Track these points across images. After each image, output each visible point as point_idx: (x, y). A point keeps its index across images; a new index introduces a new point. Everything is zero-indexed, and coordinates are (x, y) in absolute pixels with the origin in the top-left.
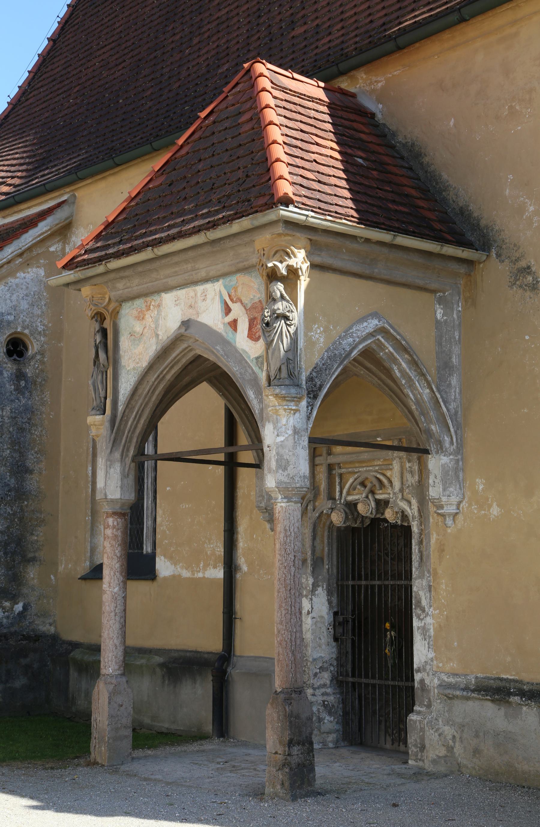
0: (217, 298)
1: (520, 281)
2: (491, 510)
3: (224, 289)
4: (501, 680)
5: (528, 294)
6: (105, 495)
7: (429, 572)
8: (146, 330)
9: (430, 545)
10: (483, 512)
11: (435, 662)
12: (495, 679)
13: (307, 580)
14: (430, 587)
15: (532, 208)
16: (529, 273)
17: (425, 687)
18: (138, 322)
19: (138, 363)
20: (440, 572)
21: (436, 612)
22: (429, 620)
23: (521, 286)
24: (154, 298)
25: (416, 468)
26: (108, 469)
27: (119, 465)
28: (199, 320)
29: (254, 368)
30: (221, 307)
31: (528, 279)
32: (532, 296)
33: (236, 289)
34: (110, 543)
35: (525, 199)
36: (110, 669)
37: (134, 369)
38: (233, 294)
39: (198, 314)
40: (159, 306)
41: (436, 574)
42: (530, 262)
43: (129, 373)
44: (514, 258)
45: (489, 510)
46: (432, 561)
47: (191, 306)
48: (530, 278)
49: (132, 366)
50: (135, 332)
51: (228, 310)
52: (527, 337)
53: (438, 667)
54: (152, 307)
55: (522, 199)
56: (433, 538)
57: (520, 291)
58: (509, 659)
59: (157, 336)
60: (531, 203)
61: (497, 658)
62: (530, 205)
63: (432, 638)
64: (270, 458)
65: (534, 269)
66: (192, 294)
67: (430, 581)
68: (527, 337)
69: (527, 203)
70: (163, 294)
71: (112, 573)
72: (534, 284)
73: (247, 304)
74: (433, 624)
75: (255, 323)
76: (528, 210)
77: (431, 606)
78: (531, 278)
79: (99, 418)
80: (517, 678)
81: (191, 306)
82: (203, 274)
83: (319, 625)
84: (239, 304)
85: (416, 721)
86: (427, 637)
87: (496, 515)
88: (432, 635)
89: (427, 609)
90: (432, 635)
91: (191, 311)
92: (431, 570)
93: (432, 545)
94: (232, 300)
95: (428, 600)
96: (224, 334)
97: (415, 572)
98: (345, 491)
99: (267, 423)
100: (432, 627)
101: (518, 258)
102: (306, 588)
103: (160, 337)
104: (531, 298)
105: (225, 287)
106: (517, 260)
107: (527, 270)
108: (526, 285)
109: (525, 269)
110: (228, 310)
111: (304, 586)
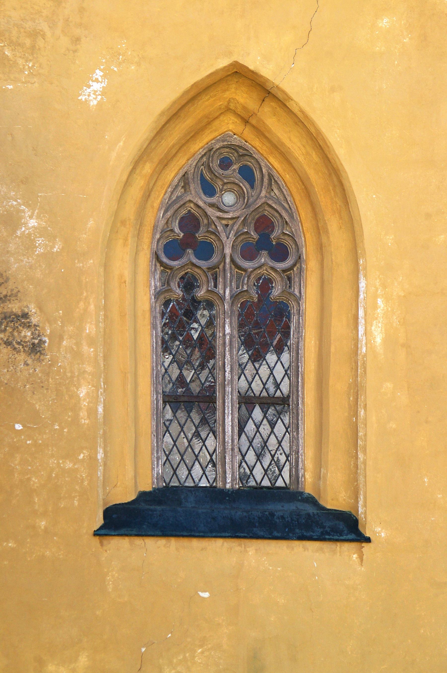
1: (7, 334)
5: (22, 357)
15: (33, 223)
31: (23, 334)
32: (29, 362)
35: (20, 205)
42: (27, 307)
52: (18, 427)
55: (15, 203)
60: (33, 213)
62: (31, 217)
65: (34, 320)
68: (18, 427)
69: (23, 211)
72: (33, 344)
76: (26, 224)
78: (29, 334)
101: (6, 296)
104: (28, 365)
108: (19, 343)
109: (17, 316)
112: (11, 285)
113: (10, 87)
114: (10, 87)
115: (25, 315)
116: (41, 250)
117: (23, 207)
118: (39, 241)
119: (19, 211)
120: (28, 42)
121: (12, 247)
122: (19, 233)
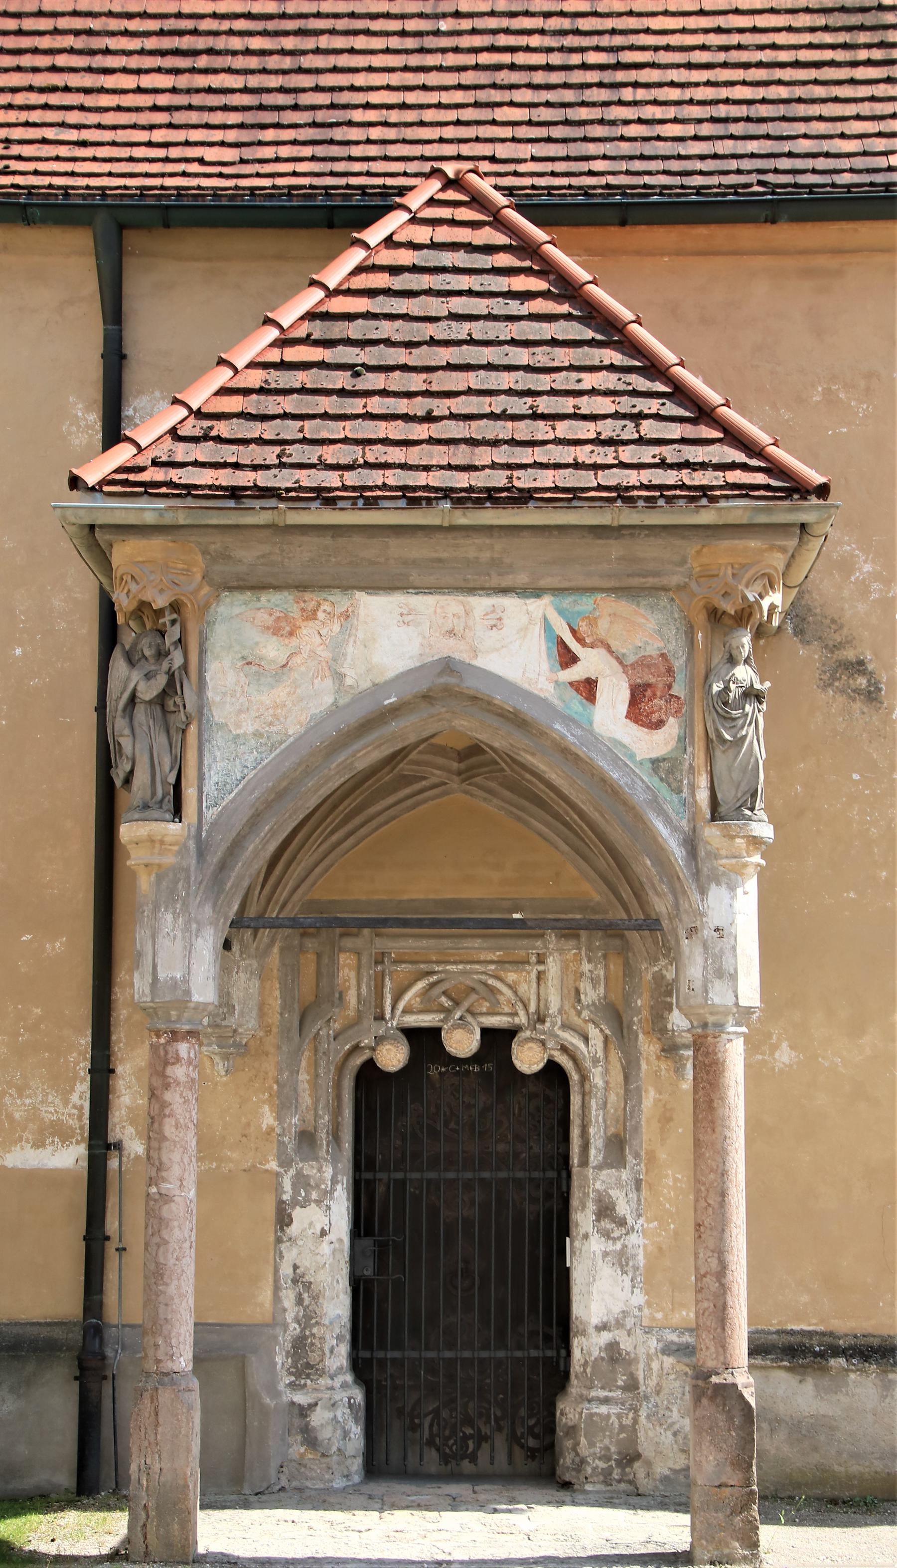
0: (537, 630)
2: (777, 1055)
3: (556, 615)
4: (792, 1333)
5: (857, 706)
6: (188, 992)
7: (637, 1156)
8: (297, 660)
9: (640, 1110)
10: (760, 1057)
11: (646, 1311)
12: (778, 1332)
13: (320, 1170)
14: (638, 1184)
15: (867, 568)
16: (863, 673)
17: (620, 1354)
18: (275, 638)
19: (271, 724)
20: (662, 1156)
21: (651, 1225)
22: (634, 1239)
23: (843, 691)
24: (331, 598)
25: (602, 973)
26: (194, 938)
27: (212, 931)
28: (479, 662)
29: (645, 778)
30: (548, 649)
32: (865, 710)
33: (592, 622)
34: (181, 1095)
35: (854, 549)
36: (182, 1359)
37: (257, 734)
38: (583, 628)
39: (475, 652)
40: (346, 616)
41: (652, 1158)
42: (863, 653)
43: (242, 740)
44: (831, 643)
45: (772, 1054)
46: (644, 1138)
47: (451, 633)
48: (862, 681)
49: (248, 727)
50: (261, 659)
51: (568, 658)
52: (856, 777)
53: (653, 1319)
54: (321, 615)
56: (647, 1098)
57: (841, 699)
58: (805, 1298)
59: (339, 677)
61: (780, 1297)
62: (865, 562)
63: (641, 1270)
64: (722, 951)
65: (870, 667)
66: (459, 610)
67: (639, 1172)
68: (856, 777)
69: (858, 556)
70: (362, 597)
71: (186, 1160)
72: (869, 692)
73: (624, 655)
74: (645, 1246)
75: (649, 693)
76: (860, 569)
77: (639, 1216)
79: (174, 828)
80: (821, 1328)
81: (451, 633)
82: (522, 579)
83: (338, 1256)
84: (603, 651)
85: (608, 1416)
86: (629, 1269)
87: (787, 1062)
88: (641, 1265)
89: (630, 1221)
90: (641, 1265)
91: (452, 642)
92: (643, 1153)
93: (645, 1110)
94: (580, 640)
95: (634, 1205)
96: (556, 702)
97: (595, 1157)
98: (401, 1005)
99: (713, 886)
100: (641, 1251)
101: (840, 643)
102: (318, 1186)
103: (349, 681)
104: (863, 713)
105: (561, 612)
106: (837, 647)
107: (859, 666)
110: (568, 658)
111: (312, 1183)
112: (845, 631)
113: (845, 430)
114: (845, 430)
115: (861, 663)
116: (874, 596)
117: (857, 552)
118: (875, 586)
119: (853, 556)
120: (862, 384)
121: (846, 593)
122: (853, 579)
